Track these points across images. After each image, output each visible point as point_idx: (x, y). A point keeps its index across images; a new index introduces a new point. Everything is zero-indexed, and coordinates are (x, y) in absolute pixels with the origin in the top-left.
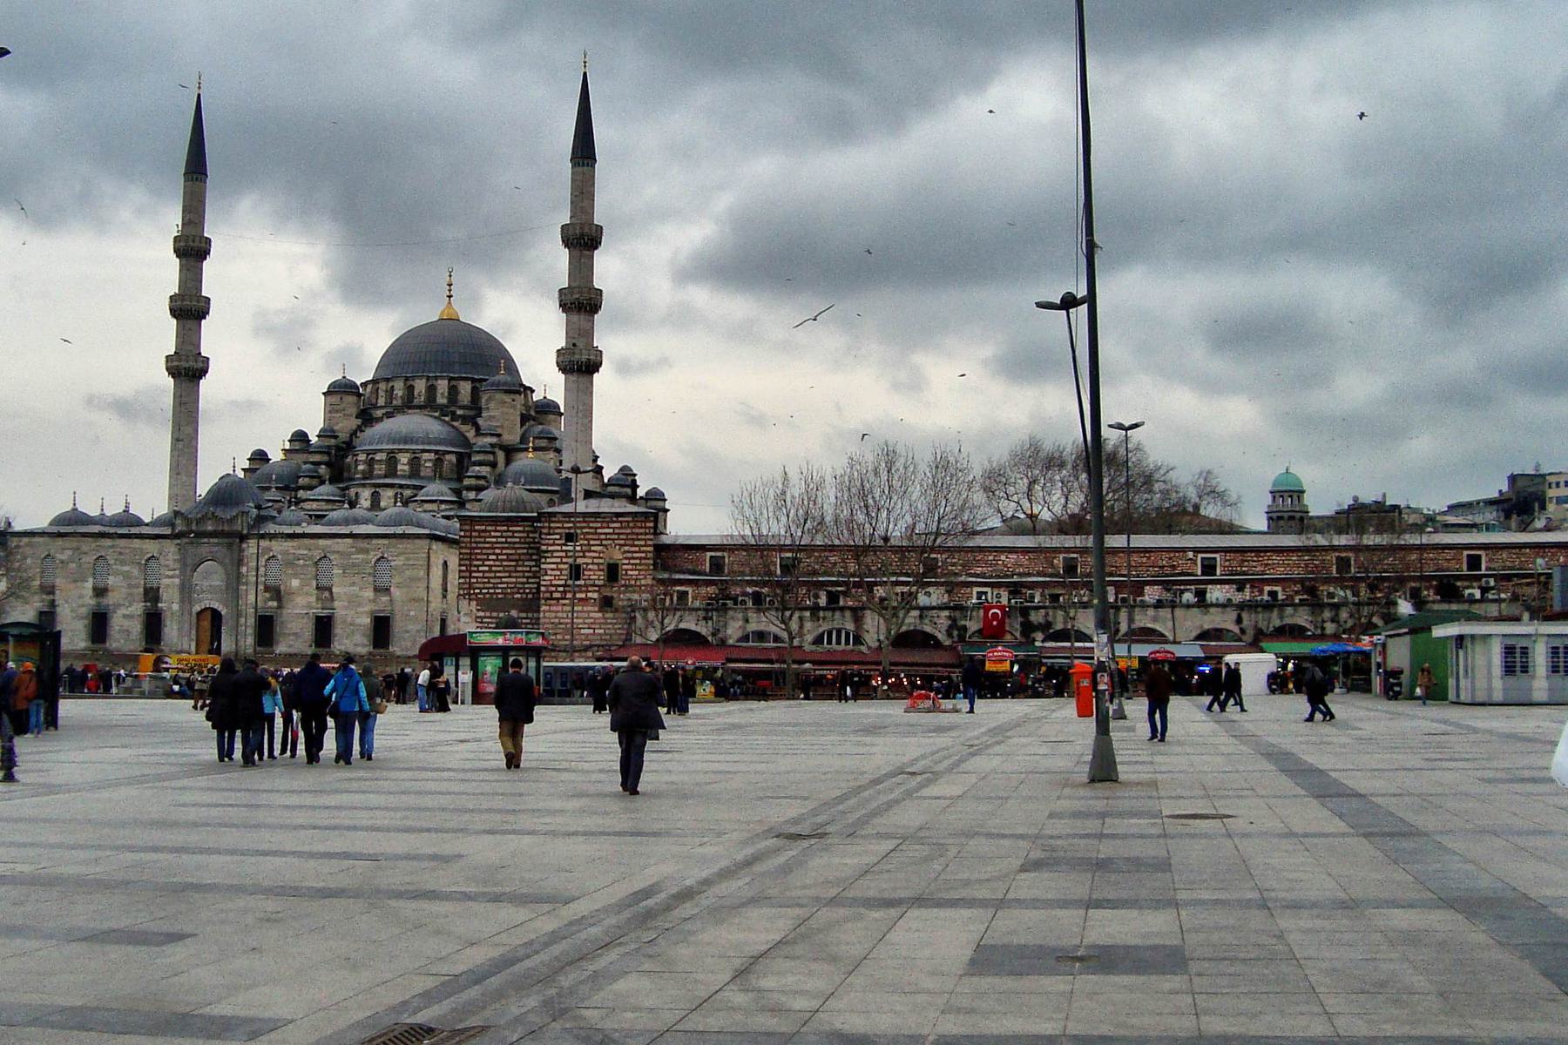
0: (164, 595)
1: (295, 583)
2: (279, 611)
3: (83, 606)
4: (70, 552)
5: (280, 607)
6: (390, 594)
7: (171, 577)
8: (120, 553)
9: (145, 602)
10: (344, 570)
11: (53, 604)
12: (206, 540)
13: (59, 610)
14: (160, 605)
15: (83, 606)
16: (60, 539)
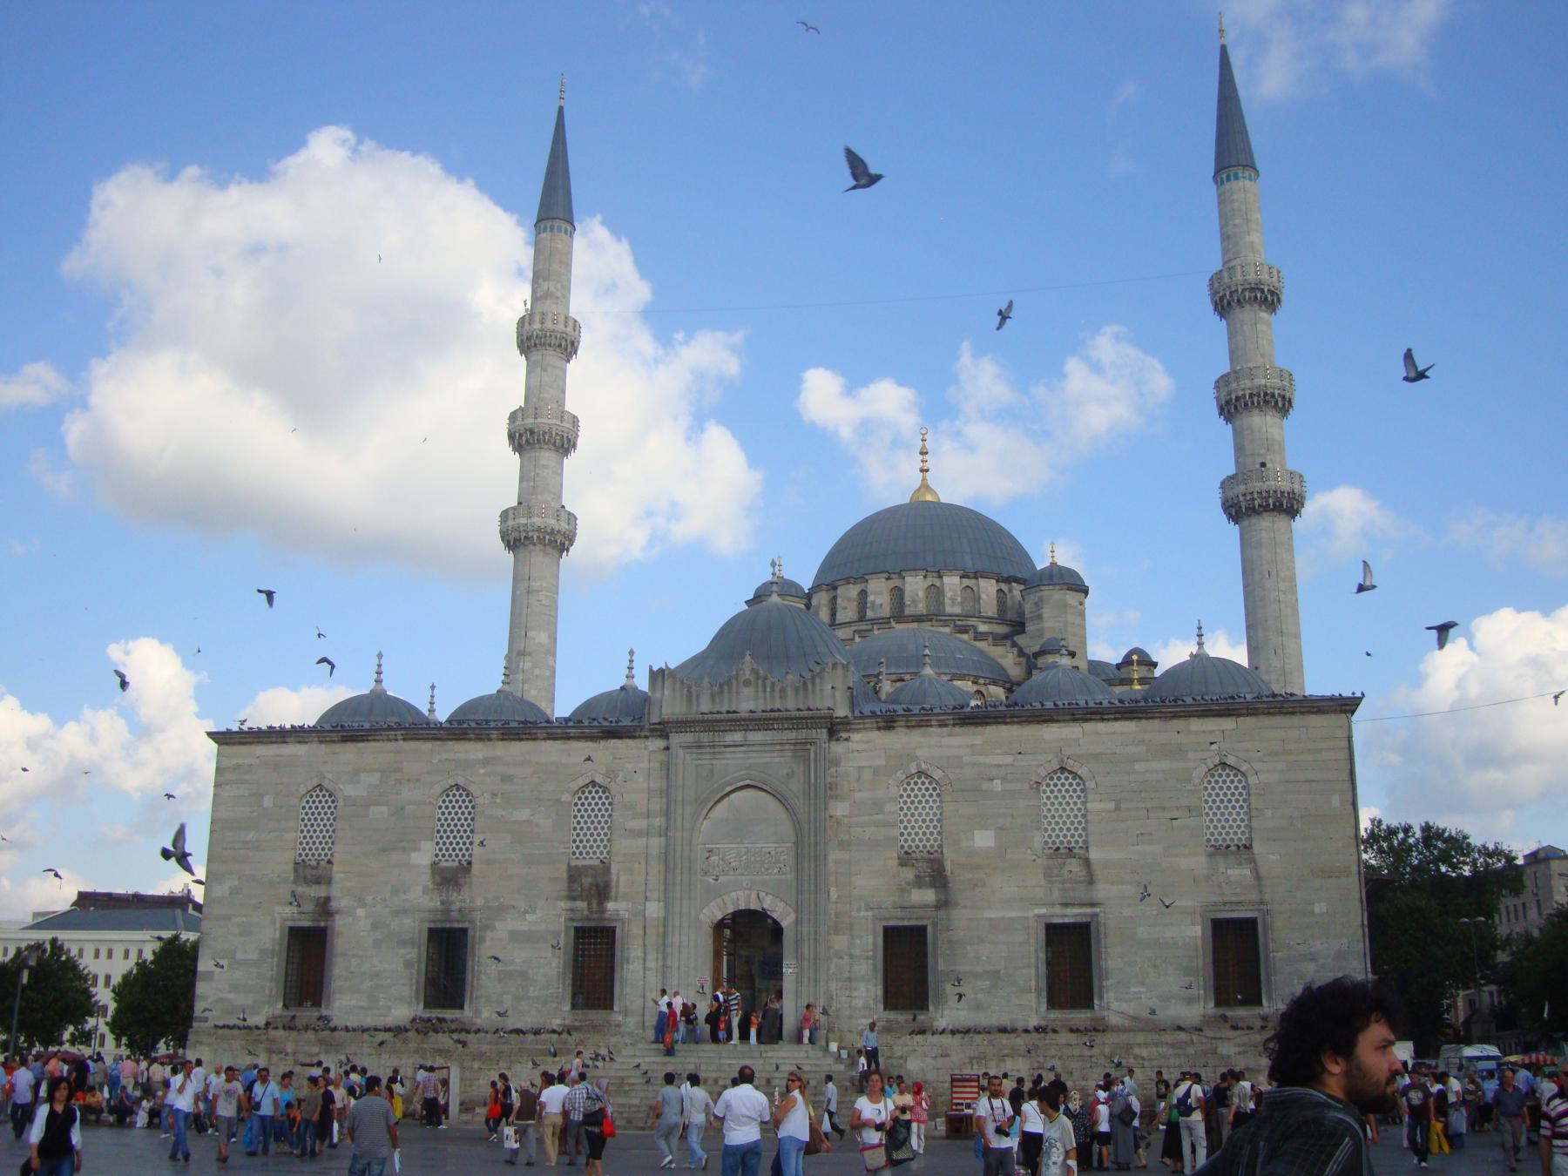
0: (621, 878)
1: (984, 839)
2: (942, 914)
3: (404, 911)
4: (375, 779)
5: (944, 904)
6: (1253, 860)
7: (639, 834)
8: (507, 779)
9: (573, 899)
10: (1118, 803)
11: (324, 908)
12: (737, 737)
13: (340, 923)
14: (611, 906)
15: (404, 911)
16: (350, 746)
